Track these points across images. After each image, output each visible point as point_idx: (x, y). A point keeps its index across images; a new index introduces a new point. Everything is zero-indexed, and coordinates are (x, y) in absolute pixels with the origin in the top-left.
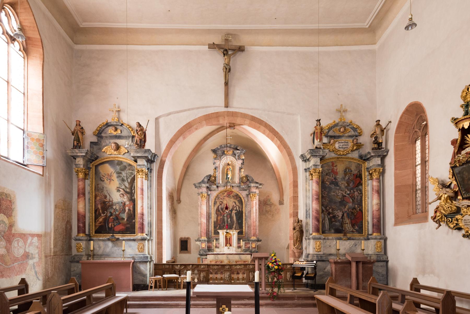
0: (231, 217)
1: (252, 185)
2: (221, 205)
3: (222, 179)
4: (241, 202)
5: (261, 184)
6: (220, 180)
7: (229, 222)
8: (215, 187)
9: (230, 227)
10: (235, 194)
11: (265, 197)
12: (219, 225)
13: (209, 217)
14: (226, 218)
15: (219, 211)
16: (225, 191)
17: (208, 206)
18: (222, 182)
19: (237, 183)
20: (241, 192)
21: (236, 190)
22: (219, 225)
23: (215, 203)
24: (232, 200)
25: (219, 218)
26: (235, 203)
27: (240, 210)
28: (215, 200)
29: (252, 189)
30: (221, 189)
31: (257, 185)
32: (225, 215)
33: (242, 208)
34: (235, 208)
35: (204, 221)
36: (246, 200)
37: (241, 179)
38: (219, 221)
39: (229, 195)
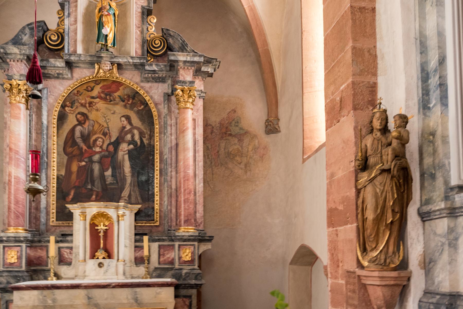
0: (117, 167)
1: (181, 57)
2: (80, 123)
3: (86, 41)
4: (147, 116)
5: (208, 61)
6: (77, 44)
7: (109, 180)
8: (60, 63)
9: (110, 195)
10: (127, 91)
11: (224, 115)
12: (74, 189)
13: (37, 158)
14: (96, 168)
15: (74, 143)
16: (97, 82)
17: (36, 129)
18: (86, 50)
19: (133, 54)
20: (147, 85)
21: (131, 79)
22: (74, 189)
23: (62, 118)
24: (119, 109)
25: (74, 168)
26: (128, 118)
27: (146, 141)
28: (63, 106)
29: (181, 72)
30: (82, 74)
31: (196, 59)
32: (96, 158)
33: (151, 137)
34: (129, 137)
35: (19, 172)
36: (164, 111)
37: (148, 48)
38: (74, 177)
39: (109, 94)
